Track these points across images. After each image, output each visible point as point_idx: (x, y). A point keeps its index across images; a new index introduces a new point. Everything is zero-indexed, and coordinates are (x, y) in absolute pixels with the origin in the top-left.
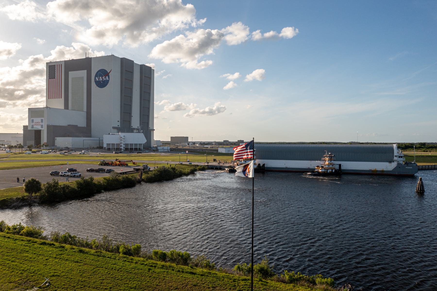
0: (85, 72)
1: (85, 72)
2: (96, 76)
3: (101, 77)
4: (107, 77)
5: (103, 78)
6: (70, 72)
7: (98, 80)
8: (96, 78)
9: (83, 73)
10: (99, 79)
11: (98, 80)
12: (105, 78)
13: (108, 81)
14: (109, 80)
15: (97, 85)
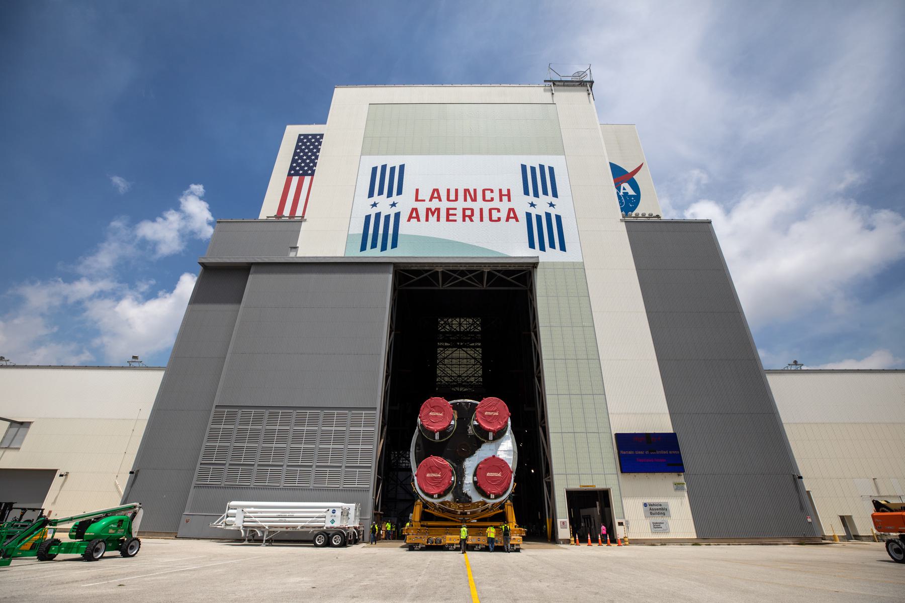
4: (626, 185)
14: (637, 198)
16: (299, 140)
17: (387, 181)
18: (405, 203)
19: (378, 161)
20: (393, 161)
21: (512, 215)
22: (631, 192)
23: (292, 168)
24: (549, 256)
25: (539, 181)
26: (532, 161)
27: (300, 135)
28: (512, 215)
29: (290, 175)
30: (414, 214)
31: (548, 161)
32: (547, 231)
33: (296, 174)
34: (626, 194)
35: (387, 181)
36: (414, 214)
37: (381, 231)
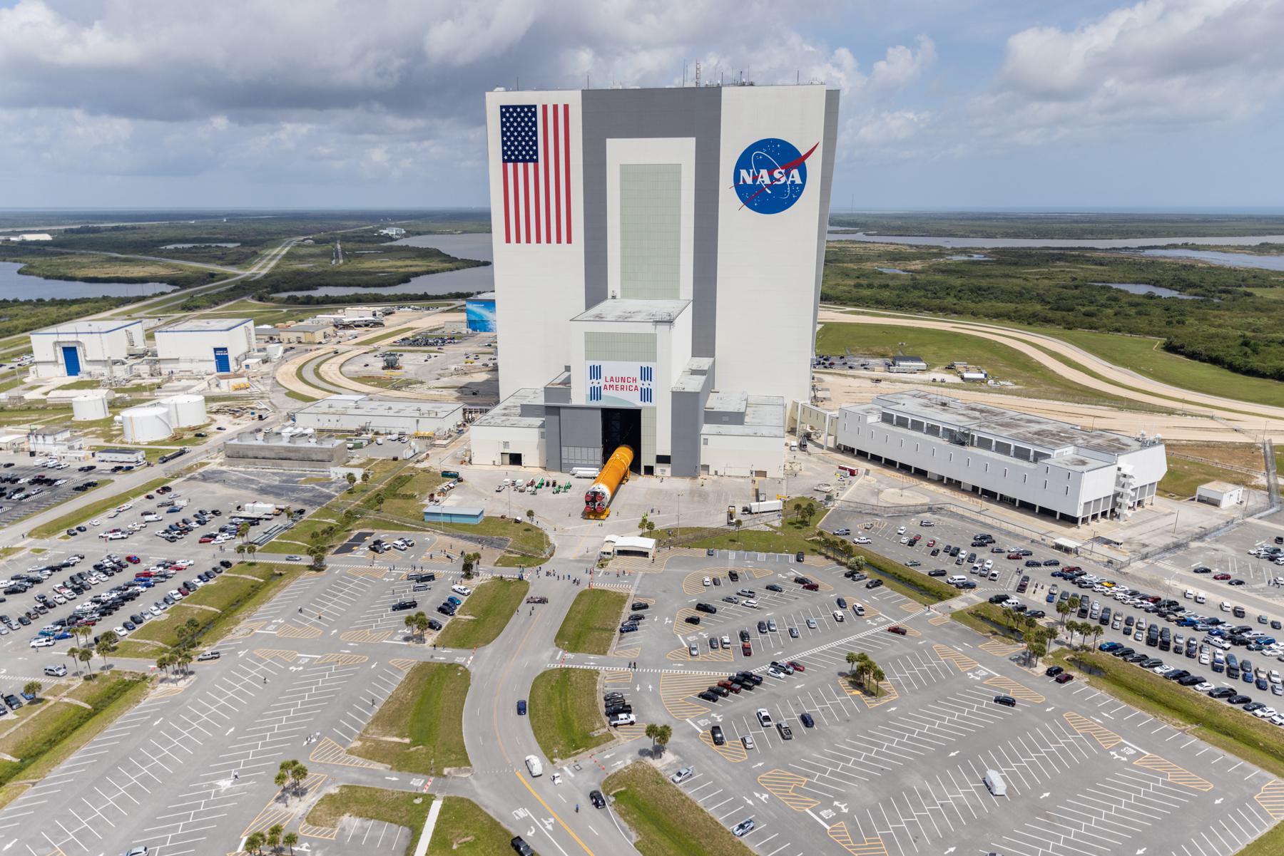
0: (689, 144)
1: (689, 144)
2: (743, 162)
3: (764, 172)
4: (795, 172)
5: (776, 174)
6: (612, 144)
7: (749, 181)
8: (743, 173)
9: (678, 152)
10: (755, 178)
11: (749, 181)
12: (787, 174)
13: (797, 190)
14: (802, 187)
15: (748, 202)
16: (503, 115)
17: (595, 372)
18: (602, 382)
19: (592, 363)
20: (597, 364)
21: (636, 388)
22: (798, 181)
23: (504, 153)
24: (647, 404)
25: (646, 374)
26: (645, 365)
27: (502, 107)
28: (636, 388)
29: (505, 161)
30: (605, 387)
31: (650, 365)
32: (646, 395)
33: (509, 160)
34: (793, 182)
35: (595, 372)
36: (605, 387)
37: (595, 394)
